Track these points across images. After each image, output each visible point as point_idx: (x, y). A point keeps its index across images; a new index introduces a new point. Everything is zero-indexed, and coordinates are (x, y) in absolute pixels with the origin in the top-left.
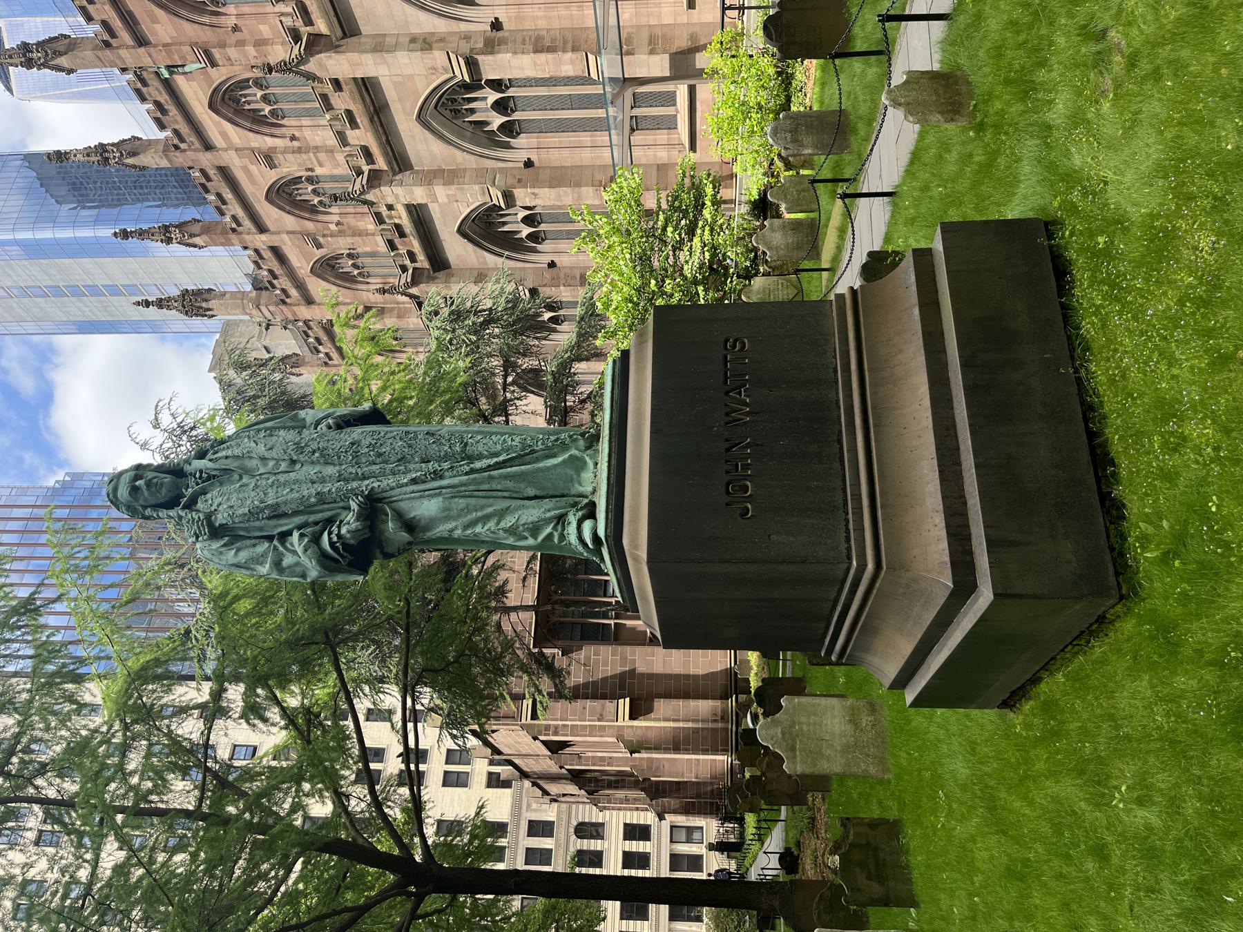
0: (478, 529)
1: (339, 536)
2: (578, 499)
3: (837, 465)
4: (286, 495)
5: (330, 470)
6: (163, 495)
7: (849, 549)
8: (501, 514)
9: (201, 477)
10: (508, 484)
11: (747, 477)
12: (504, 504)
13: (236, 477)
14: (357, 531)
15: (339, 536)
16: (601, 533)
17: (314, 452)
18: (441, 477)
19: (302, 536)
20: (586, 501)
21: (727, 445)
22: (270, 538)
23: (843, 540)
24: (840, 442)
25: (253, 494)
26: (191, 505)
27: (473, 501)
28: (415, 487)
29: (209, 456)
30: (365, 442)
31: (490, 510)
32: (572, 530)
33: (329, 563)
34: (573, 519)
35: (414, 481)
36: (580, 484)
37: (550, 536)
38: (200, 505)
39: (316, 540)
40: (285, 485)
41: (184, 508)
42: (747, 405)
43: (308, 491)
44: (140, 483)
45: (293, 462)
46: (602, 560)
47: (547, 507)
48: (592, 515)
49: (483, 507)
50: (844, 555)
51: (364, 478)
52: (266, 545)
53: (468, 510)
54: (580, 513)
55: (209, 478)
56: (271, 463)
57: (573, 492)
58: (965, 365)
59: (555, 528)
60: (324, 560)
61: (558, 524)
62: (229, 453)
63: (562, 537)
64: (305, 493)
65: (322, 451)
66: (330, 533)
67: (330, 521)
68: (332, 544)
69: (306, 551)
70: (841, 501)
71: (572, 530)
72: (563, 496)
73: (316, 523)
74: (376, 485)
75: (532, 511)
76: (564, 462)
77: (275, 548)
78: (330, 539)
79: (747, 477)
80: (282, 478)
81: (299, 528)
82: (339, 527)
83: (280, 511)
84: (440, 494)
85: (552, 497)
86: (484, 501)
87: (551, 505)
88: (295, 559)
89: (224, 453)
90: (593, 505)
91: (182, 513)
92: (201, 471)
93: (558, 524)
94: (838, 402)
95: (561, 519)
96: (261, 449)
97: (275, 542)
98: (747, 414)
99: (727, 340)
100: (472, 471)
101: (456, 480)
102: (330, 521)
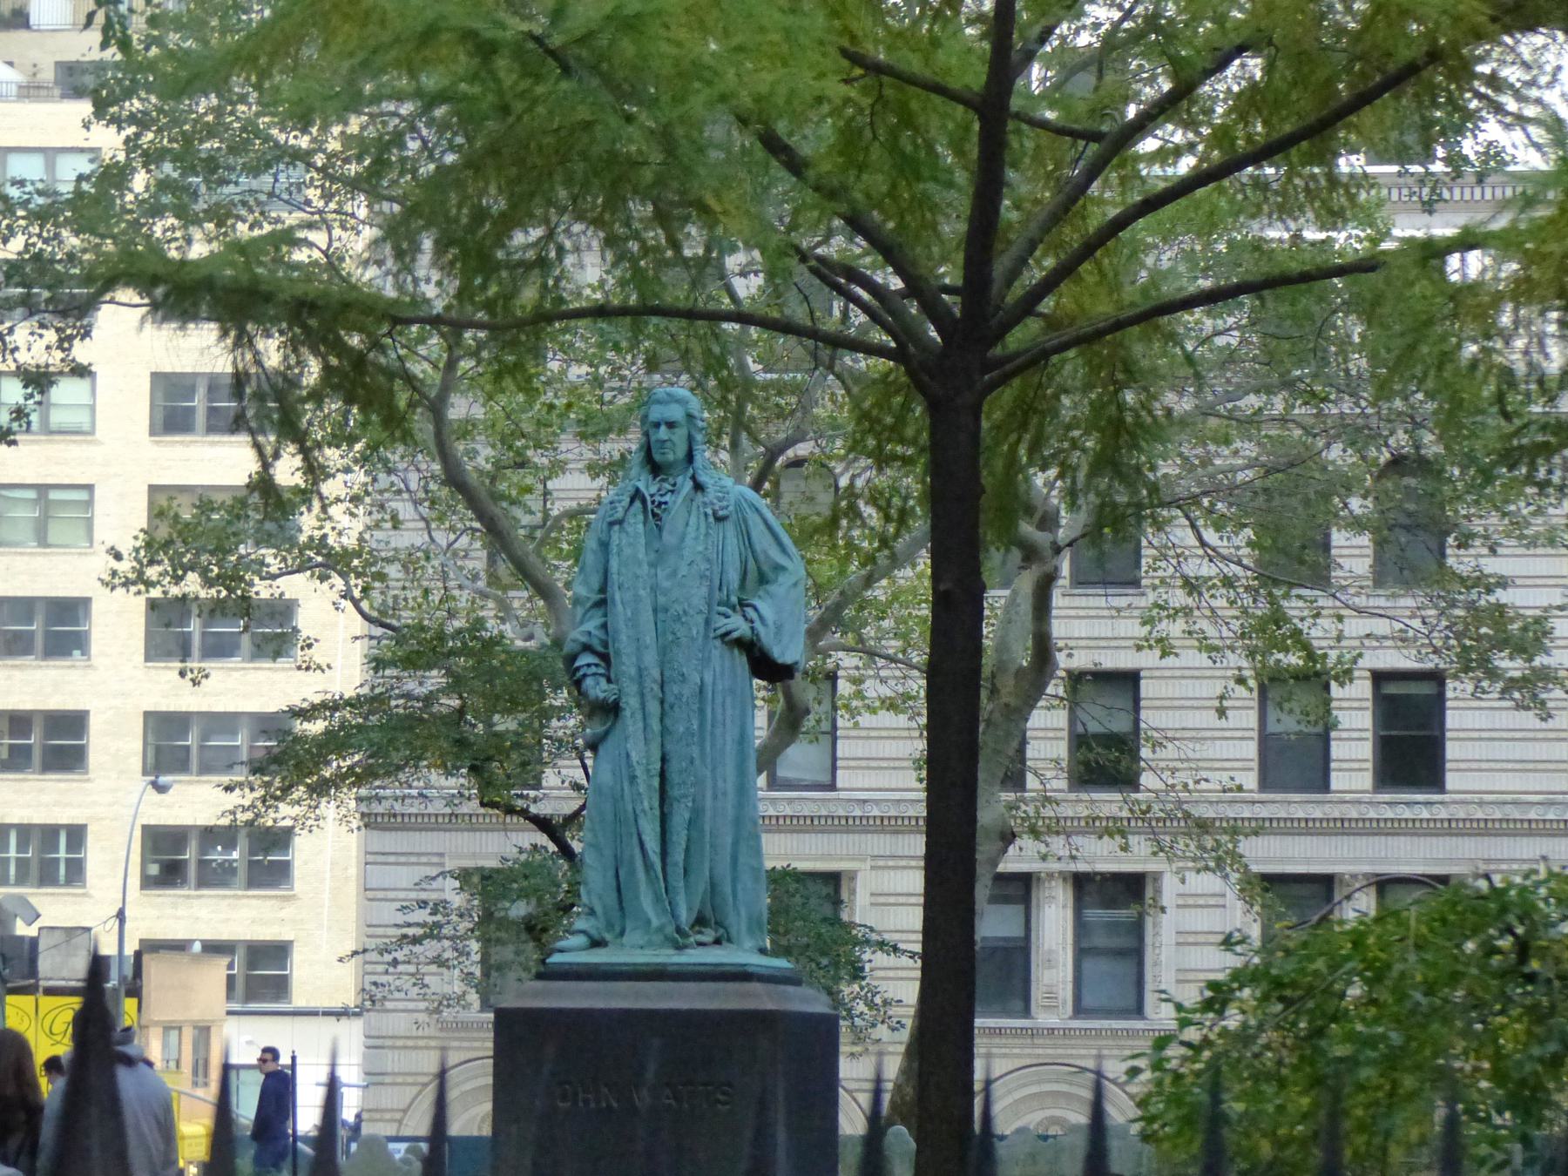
1: (585, 676)
2: (618, 929)
4: (620, 612)
5: (650, 658)
6: (657, 457)
11: (575, 1103)
12: (608, 852)
13: (656, 545)
15: (585, 676)
20: (608, 937)
22: (603, 589)
27: (610, 817)
35: (628, 755)
39: (587, 648)
40: (636, 612)
43: (624, 642)
44: (663, 428)
45: (667, 610)
48: (596, 943)
51: (642, 695)
54: (593, 932)
62: (691, 530)
66: (589, 665)
67: (605, 658)
68: (578, 669)
72: (622, 908)
73: (605, 644)
74: (627, 713)
85: (620, 902)
89: (693, 520)
95: (592, 912)
96: (683, 570)
97: (596, 597)
101: (627, 797)
102: (605, 658)
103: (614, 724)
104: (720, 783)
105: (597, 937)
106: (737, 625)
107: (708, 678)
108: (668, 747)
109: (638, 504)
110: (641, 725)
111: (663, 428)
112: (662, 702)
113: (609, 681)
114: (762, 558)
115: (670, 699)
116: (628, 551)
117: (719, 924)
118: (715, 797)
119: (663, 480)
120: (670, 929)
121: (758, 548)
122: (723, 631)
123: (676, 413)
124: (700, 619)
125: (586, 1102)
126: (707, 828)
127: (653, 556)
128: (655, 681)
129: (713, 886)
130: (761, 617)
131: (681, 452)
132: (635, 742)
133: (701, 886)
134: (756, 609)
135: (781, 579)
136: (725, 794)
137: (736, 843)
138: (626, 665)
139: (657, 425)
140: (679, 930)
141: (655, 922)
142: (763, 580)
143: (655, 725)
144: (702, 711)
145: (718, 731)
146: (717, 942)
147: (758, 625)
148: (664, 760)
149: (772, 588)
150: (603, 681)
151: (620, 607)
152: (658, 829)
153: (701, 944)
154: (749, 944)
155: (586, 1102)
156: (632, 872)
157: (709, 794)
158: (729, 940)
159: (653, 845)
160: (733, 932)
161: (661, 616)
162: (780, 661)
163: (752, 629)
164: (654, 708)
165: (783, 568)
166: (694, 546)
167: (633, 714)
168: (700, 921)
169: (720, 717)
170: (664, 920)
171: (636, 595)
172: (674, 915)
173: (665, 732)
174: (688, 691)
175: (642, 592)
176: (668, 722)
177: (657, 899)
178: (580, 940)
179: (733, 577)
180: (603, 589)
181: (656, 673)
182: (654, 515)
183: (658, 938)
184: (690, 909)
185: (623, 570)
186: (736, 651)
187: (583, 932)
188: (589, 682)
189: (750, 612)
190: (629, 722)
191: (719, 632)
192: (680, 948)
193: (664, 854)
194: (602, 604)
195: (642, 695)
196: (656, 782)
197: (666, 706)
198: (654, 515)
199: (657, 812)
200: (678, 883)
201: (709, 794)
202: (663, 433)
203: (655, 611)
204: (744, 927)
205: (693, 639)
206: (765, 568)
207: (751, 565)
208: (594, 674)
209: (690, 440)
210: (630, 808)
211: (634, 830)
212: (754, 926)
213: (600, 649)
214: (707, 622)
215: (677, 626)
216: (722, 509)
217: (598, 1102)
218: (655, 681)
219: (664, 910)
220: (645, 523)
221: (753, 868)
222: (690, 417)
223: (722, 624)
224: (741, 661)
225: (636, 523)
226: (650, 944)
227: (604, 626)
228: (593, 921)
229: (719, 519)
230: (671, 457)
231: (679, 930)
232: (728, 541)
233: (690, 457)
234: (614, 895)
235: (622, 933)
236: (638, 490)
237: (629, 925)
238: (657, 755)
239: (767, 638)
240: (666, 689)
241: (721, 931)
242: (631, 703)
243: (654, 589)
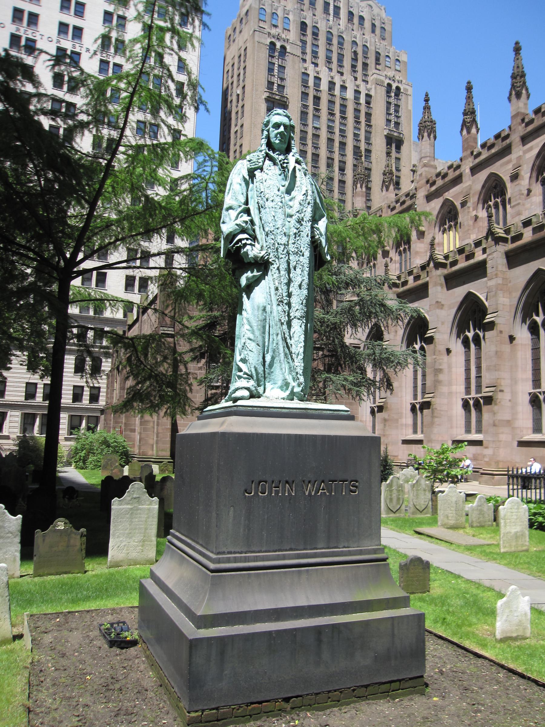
0: (247, 327)
1: (245, 245)
3: (276, 548)
7: (224, 553)
9: (284, 163)
11: (270, 492)
14: (248, 255)
16: (239, 403)
19: (246, 222)
21: (290, 481)
23: (229, 550)
24: (291, 549)
26: (267, 156)
29: (298, 167)
32: (243, 383)
33: (230, 238)
34: (251, 384)
37: (240, 370)
38: (267, 162)
39: (243, 231)
41: (267, 153)
46: (227, 401)
48: (252, 396)
50: (220, 550)
52: (243, 200)
55: (283, 167)
57: (267, 384)
58: (335, 627)
59: (245, 373)
60: (231, 237)
61: (248, 375)
63: (240, 377)
66: (247, 239)
68: (240, 240)
69: (237, 225)
70: (254, 549)
71: (243, 383)
73: (254, 231)
77: (240, 206)
78: (243, 239)
79: (270, 492)
81: (252, 222)
82: (250, 244)
83: (262, 209)
88: (234, 218)
90: (259, 397)
91: (263, 152)
92: (287, 163)
93: (248, 375)
94: (317, 549)
95: (250, 377)
97: (243, 206)
99: (357, 481)
125: (277, 492)
155: (277, 492)
178: (246, 393)
180: (247, 203)
187: (248, 389)
188: (248, 247)
213: (251, 232)
217: (284, 493)
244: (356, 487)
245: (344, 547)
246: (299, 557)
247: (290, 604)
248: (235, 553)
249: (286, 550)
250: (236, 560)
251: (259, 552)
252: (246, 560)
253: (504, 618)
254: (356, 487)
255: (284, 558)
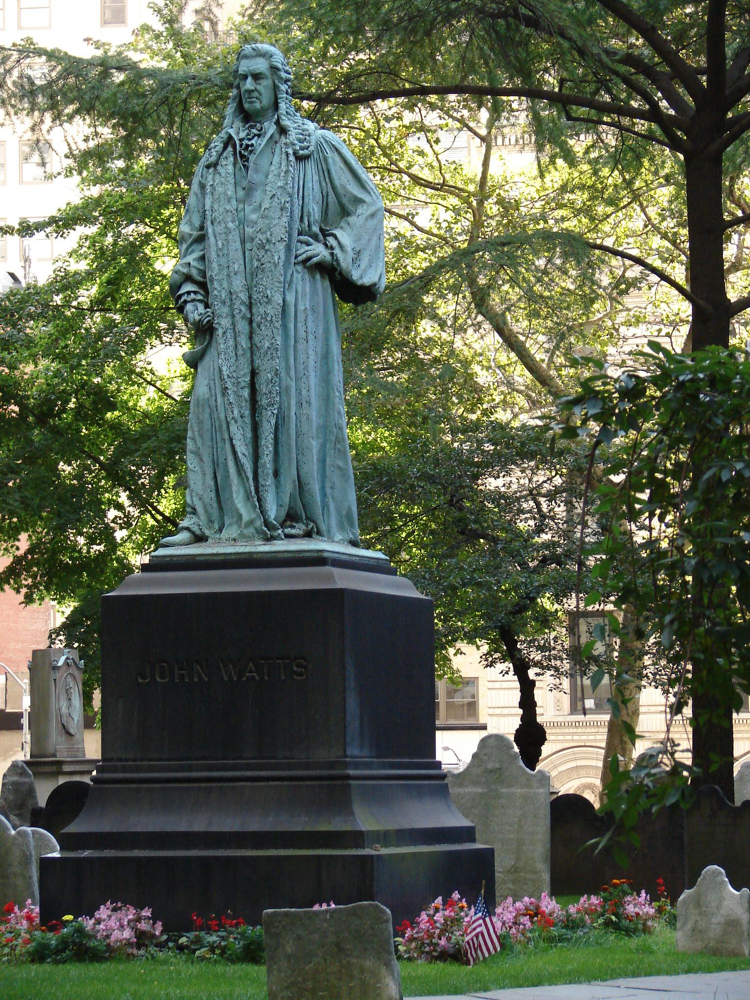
1: (186, 302)
5: (238, 284)
6: (246, 106)
7: (112, 760)
8: (197, 454)
10: (221, 460)
13: (245, 184)
15: (186, 302)
17: (258, 260)
18: (223, 395)
20: (207, 532)
25: (221, 209)
27: (207, 425)
28: (217, 370)
30: (270, 310)
31: (199, 443)
35: (220, 370)
36: (231, 524)
39: (188, 278)
42: (240, 677)
44: (249, 79)
47: (205, 496)
48: (200, 539)
49: (201, 436)
53: (200, 422)
54: (195, 529)
56: (254, 217)
57: (226, 518)
64: (215, 265)
65: (261, 268)
66: (189, 293)
67: (203, 286)
72: (221, 508)
73: (203, 273)
74: (220, 332)
75: (200, 483)
76: (237, 510)
78: (184, 294)
80: (235, 237)
84: (212, 396)
86: (207, 436)
87: (207, 500)
94: (242, 758)
97: (195, 234)
98: (230, 677)
100: (228, 424)
101: (221, 409)
102: (203, 286)
103: (209, 344)
104: (304, 392)
105: (198, 532)
106: (319, 251)
107: (290, 298)
108: (257, 362)
109: (230, 149)
110: (231, 342)
111: (249, 79)
112: (251, 322)
113: (207, 306)
114: (340, 190)
115: (257, 319)
116: (220, 189)
117: (310, 519)
118: (300, 405)
119: (252, 127)
120: (259, 523)
121: (337, 182)
122: (304, 256)
123: (261, 65)
124: (281, 247)
126: (293, 433)
127: (241, 193)
128: (243, 303)
129: (301, 485)
130: (339, 243)
131: (266, 99)
132: (225, 356)
133: (289, 486)
134: (336, 237)
135: (359, 211)
136: (309, 403)
137: (323, 446)
138: (218, 290)
139: (245, 77)
140: (267, 523)
141: (246, 517)
142: (345, 212)
143: (244, 342)
144: (285, 327)
145: (301, 347)
146: (308, 535)
147: (337, 251)
148: (254, 373)
149: (351, 219)
150: (201, 307)
151: (212, 239)
152: (249, 435)
153: (289, 536)
154: (338, 537)
156: (227, 476)
157: (293, 402)
158: (319, 533)
159: (243, 449)
160: (323, 527)
161: (248, 246)
162: (360, 283)
163: (332, 254)
164: (242, 326)
165: (360, 201)
166: (275, 182)
167: (224, 333)
168: (291, 517)
169: (301, 333)
170: (253, 516)
171: (226, 227)
172: (263, 512)
173: (253, 348)
174: (272, 310)
175: (230, 225)
176: (256, 339)
177: (248, 497)
179: (315, 210)
181: (244, 297)
182: (242, 156)
183: (251, 530)
184: (280, 506)
185: (216, 206)
186: (318, 276)
188: (189, 307)
189: (331, 241)
190: (221, 340)
191: (300, 258)
192: (269, 539)
193: (256, 457)
194: (201, 239)
195: (233, 316)
196: (246, 393)
197: (254, 325)
198: (242, 156)
199: (248, 420)
200: (268, 481)
201: (293, 402)
202: (249, 84)
203: (243, 242)
204: (334, 522)
205: (276, 265)
206: (345, 201)
207: (332, 198)
208: (193, 300)
209: (275, 88)
210: (223, 416)
211: (226, 437)
212: (345, 520)
214: (288, 248)
215: (262, 252)
216: (302, 149)
218: (243, 303)
219: (254, 507)
220: (235, 164)
221: (339, 467)
222: (274, 69)
223: (304, 251)
224: (323, 286)
225: (228, 165)
226: (242, 536)
227: (202, 258)
228: (195, 519)
229: (300, 158)
230: (258, 105)
231: (267, 523)
232: (309, 177)
233: (276, 106)
234: (213, 495)
235: (220, 530)
236: (230, 138)
237: (227, 521)
238: (247, 370)
239: (345, 261)
240: (254, 311)
241: (311, 525)
242: (223, 323)
243: (242, 223)
244: (305, 667)
245: (285, 758)
246: (210, 768)
247: (182, 827)
248: (126, 760)
249: (197, 759)
250: (125, 769)
251: (159, 760)
252: (138, 769)
253: (689, 926)
254: (305, 667)
255: (190, 769)
